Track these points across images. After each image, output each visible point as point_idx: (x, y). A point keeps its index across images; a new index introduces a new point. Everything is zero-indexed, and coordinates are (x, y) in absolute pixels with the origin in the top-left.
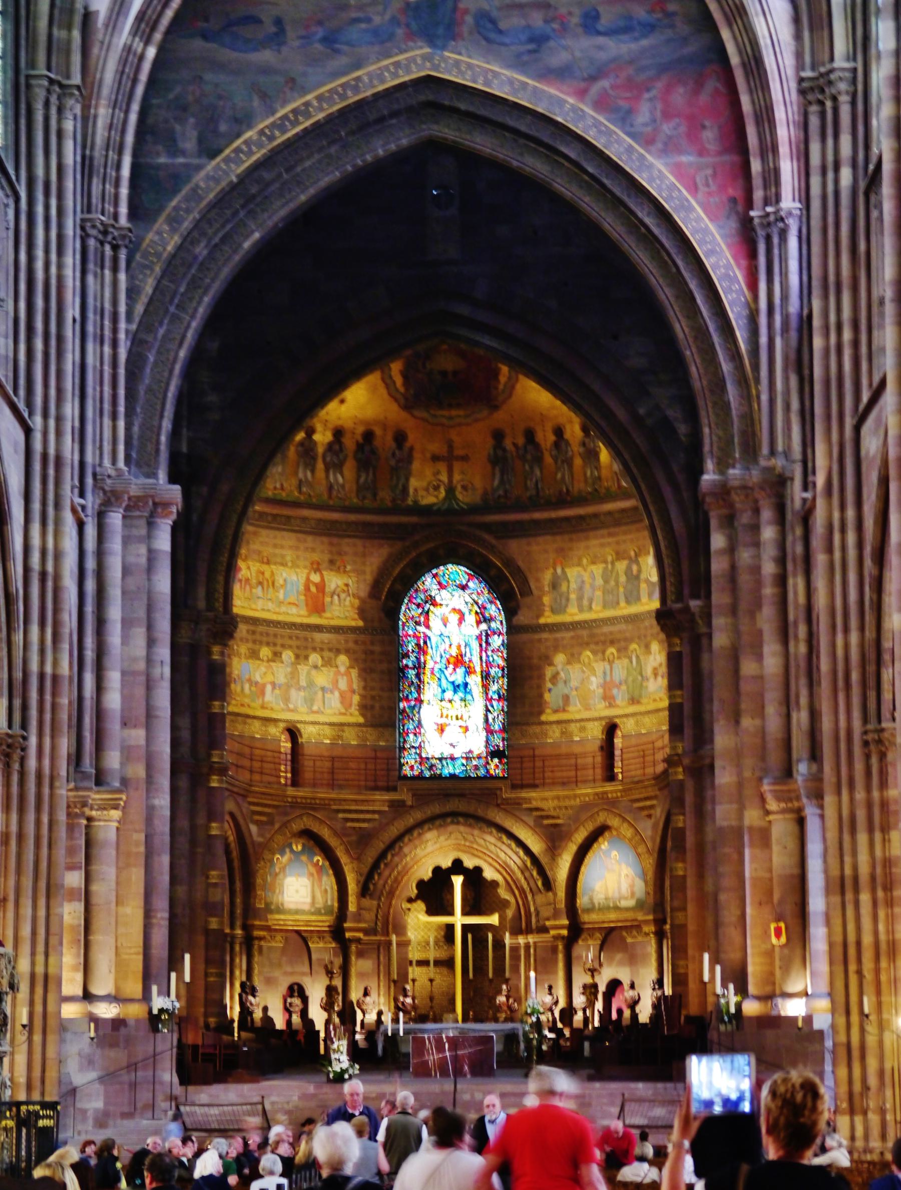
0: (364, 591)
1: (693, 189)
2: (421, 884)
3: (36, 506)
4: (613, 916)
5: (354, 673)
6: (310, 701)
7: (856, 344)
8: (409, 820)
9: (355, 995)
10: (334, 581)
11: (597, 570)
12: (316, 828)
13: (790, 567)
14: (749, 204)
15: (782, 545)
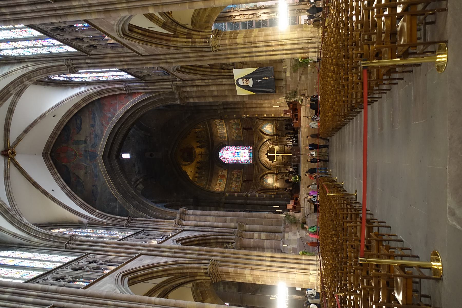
0: (222, 169)
1: (123, 105)
2: (269, 160)
3: (158, 253)
4: (275, 129)
5: (235, 171)
6: (239, 178)
7: (124, 57)
8: (259, 162)
9: (287, 172)
10: (220, 173)
11: (218, 131)
12: (260, 178)
13: (194, 84)
14: (125, 94)
15: (191, 86)
